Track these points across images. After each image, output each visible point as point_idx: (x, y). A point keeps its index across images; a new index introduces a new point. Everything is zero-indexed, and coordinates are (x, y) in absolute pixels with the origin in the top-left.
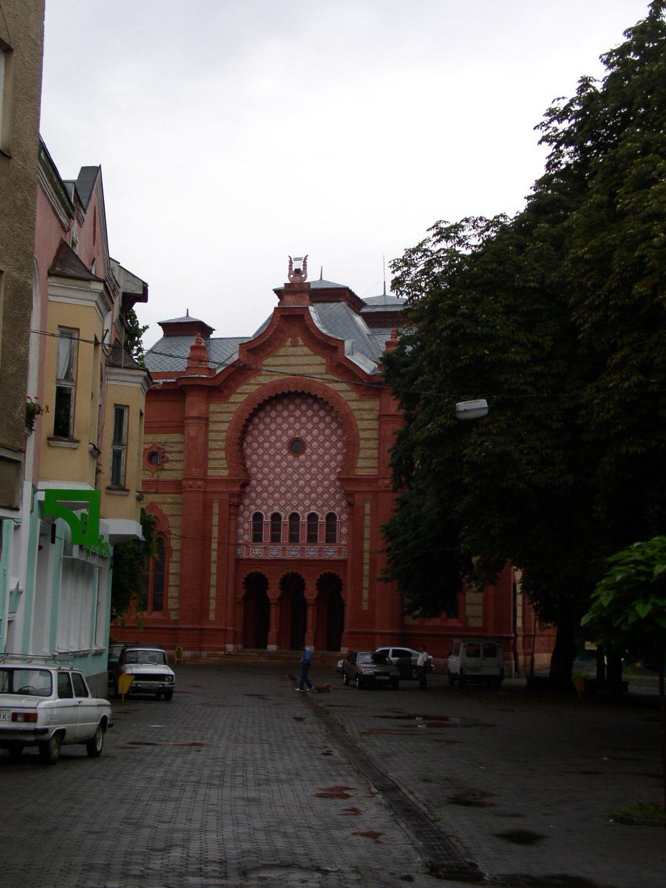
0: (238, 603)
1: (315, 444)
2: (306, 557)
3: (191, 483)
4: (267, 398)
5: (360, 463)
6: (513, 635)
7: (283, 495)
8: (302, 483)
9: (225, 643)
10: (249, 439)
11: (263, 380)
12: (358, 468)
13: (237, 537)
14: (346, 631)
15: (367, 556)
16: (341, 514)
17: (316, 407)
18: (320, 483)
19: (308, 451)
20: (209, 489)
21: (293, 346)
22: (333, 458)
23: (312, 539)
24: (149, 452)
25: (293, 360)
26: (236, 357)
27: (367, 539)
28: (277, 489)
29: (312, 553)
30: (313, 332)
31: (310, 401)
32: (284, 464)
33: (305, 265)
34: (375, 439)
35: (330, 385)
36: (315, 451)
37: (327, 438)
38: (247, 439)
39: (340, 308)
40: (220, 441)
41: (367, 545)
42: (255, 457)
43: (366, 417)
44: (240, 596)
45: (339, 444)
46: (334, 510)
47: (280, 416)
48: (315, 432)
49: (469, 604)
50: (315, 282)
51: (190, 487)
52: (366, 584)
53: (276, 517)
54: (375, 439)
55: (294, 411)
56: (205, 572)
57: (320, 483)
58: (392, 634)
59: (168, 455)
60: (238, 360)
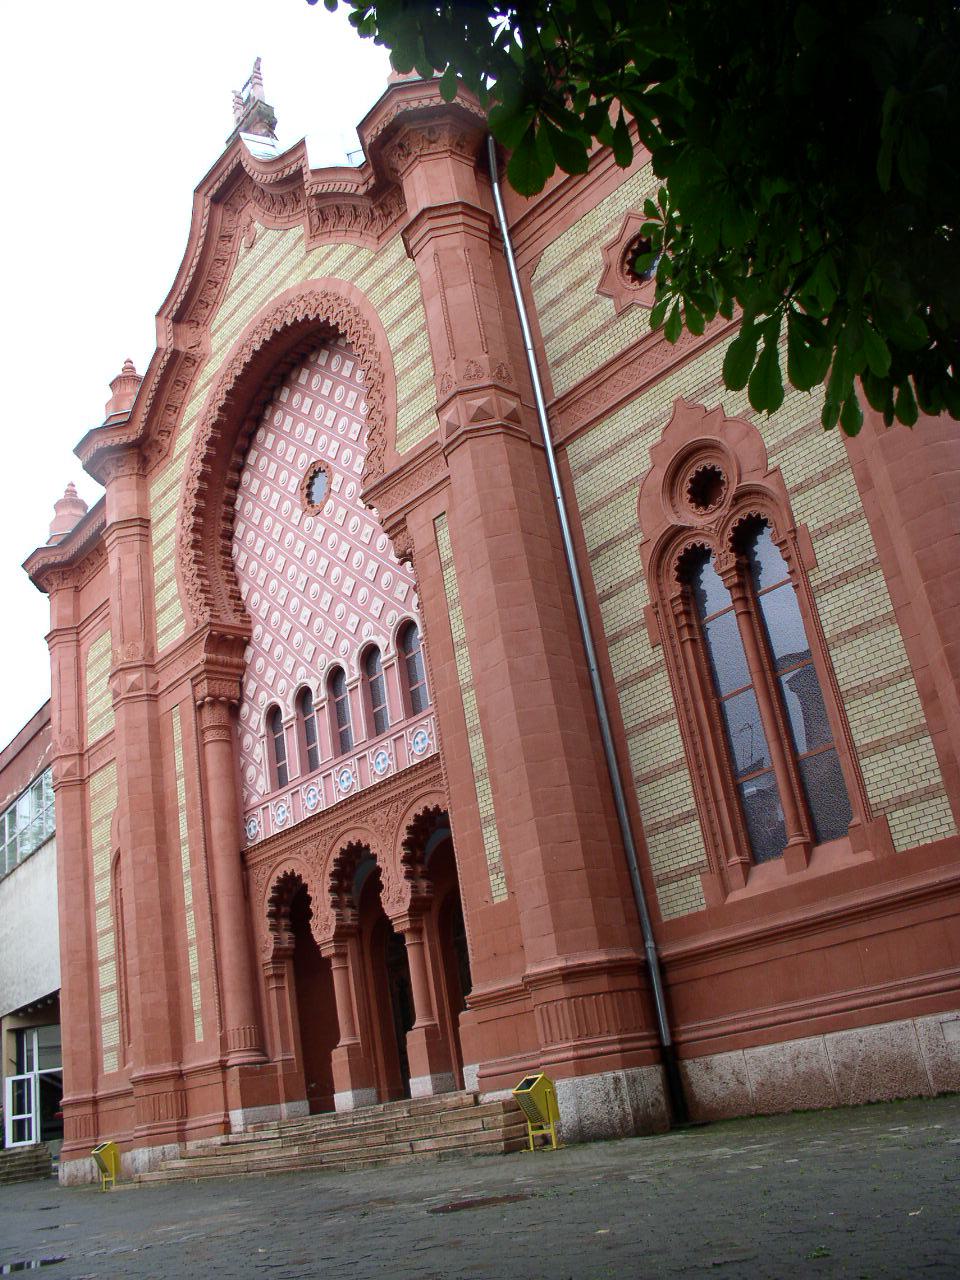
0: (268, 978)
10: (240, 529)
49: (877, 747)
56: (168, 912)
58: (568, 975)
60: (158, 350)
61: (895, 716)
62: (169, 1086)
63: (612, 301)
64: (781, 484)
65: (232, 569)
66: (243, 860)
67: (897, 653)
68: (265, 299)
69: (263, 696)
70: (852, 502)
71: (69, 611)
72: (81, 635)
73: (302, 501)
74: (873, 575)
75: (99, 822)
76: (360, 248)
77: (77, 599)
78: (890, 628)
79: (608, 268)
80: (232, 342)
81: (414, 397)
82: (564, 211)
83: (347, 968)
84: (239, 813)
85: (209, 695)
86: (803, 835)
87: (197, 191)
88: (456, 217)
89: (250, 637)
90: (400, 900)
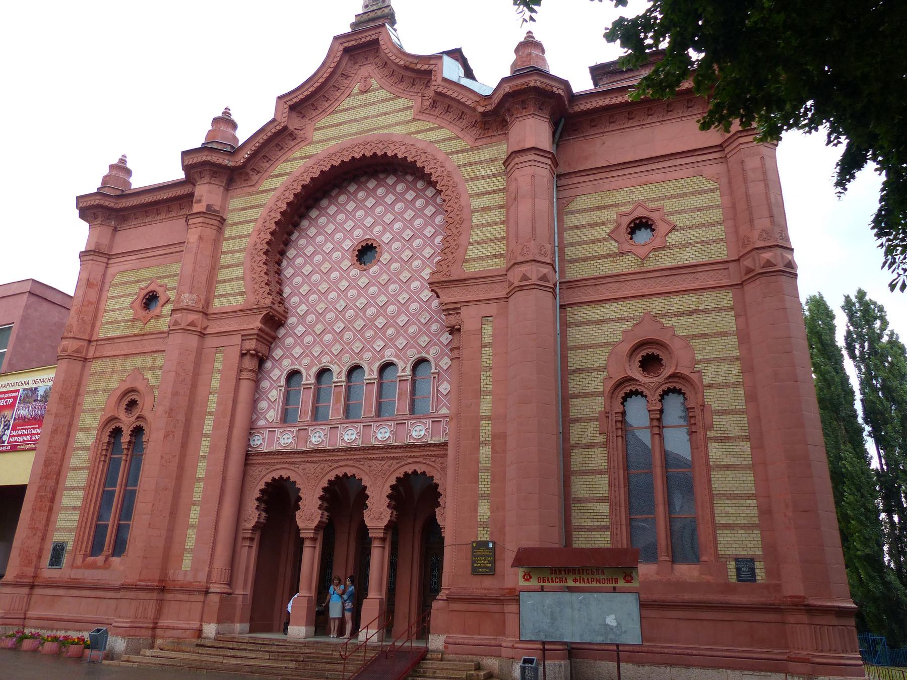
0: (244, 538)
1: (396, 245)
2: (374, 442)
5: (473, 252)
8: (371, 311)
10: (291, 253)
11: (310, 150)
12: (466, 261)
14: (442, 595)
15: (486, 428)
16: (439, 357)
17: (400, 187)
19: (385, 257)
20: (208, 331)
21: (363, 92)
24: (145, 292)
25: (361, 113)
27: (488, 393)
29: (383, 434)
30: (393, 58)
34: (501, 207)
35: (420, 136)
41: (486, 406)
42: (298, 279)
43: (483, 173)
45: (438, 239)
46: (428, 353)
49: (727, 527)
52: (484, 486)
54: (501, 207)
60: (273, 120)
61: (742, 515)
63: (617, 244)
64: (701, 379)
65: (279, 275)
66: (249, 457)
67: (749, 485)
68: (370, 130)
70: (740, 405)
71: (105, 241)
72: (111, 261)
73: (352, 257)
74: (744, 443)
75: (95, 392)
76: (458, 138)
77: (113, 235)
78: (748, 472)
79: (619, 226)
80: (334, 142)
81: (483, 243)
82: (598, 181)
83: (315, 547)
84: (251, 429)
85: (254, 350)
86: (668, 556)
87: (336, 38)
88: (547, 159)
89: (285, 322)
90: (380, 519)
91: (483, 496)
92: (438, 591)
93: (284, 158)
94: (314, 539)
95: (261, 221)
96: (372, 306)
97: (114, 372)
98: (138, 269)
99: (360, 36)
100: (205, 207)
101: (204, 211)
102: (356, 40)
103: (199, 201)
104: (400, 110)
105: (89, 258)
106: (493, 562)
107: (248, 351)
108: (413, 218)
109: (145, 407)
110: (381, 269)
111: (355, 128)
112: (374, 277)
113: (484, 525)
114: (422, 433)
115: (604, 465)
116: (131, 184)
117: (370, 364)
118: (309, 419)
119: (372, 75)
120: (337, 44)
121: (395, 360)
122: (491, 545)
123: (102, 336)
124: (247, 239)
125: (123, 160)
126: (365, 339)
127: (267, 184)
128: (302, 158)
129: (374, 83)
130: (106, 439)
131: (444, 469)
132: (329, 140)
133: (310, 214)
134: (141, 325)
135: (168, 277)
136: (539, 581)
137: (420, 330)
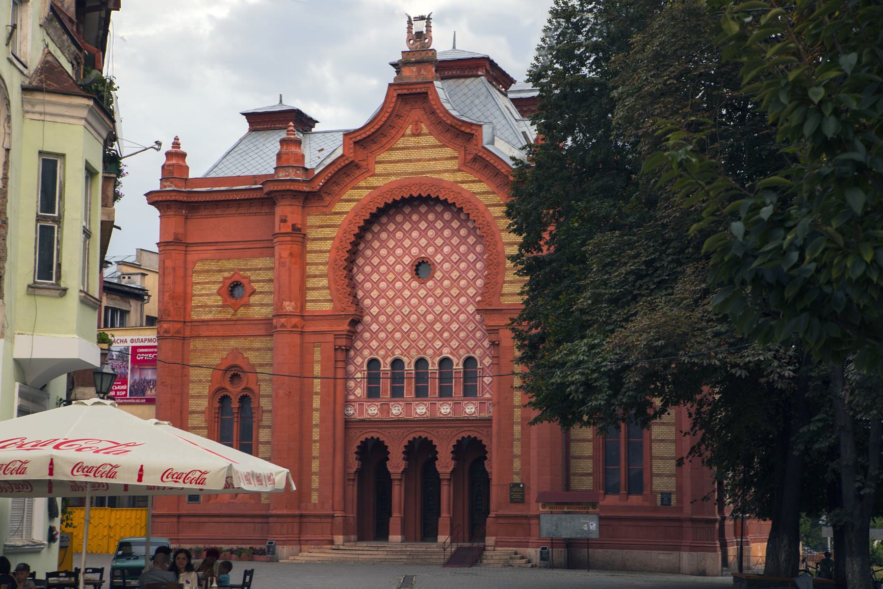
0: (348, 479)
1: (446, 266)
2: (438, 415)
3: (283, 320)
4: (382, 206)
6: (718, 517)
7: (406, 335)
8: (430, 317)
9: (332, 535)
10: (360, 261)
12: (503, 295)
13: (347, 391)
14: (492, 514)
16: (482, 357)
17: (447, 216)
18: (455, 317)
19: (438, 275)
20: (306, 329)
21: (414, 135)
22: (471, 283)
23: (445, 393)
24: (230, 281)
26: (339, 152)
28: (398, 328)
29: (445, 410)
30: (441, 115)
31: (439, 209)
32: (407, 293)
33: (428, 26)
36: (446, 276)
37: (463, 258)
38: (357, 262)
39: (479, 84)
40: (321, 264)
42: (368, 285)
44: (353, 469)
45: (479, 265)
46: (474, 353)
47: (400, 230)
48: (446, 249)
49: (658, 475)
50: (444, 53)
51: (283, 326)
52: (517, 450)
53: (397, 363)
55: (419, 222)
57: (455, 317)
59: (256, 286)
60: (343, 156)
62: (297, 520)
65: (351, 279)
68: (423, 173)
69: (366, 352)
72: (189, 249)
76: (493, 193)
80: (393, 178)
81: (513, 283)
84: (347, 403)
90: (446, 467)
91: (516, 456)
92: (488, 512)
93: (351, 185)
94: (400, 480)
95: (337, 241)
96: (430, 313)
97: (213, 350)
98: (219, 260)
99: (411, 87)
100: (291, 226)
101: (290, 230)
102: (408, 89)
103: (284, 221)
104: (447, 159)
105: (171, 248)
106: (523, 496)
107: (340, 347)
108: (459, 245)
109: (247, 381)
110: (436, 284)
111: (410, 168)
112: (430, 290)
113: (517, 474)
114: (473, 410)
115: (591, 436)
116: (187, 168)
117: (432, 358)
118: (389, 396)
119: (422, 120)
120: (392, 89)
121: (450, 356)
122: (521, 486)
123: (195, 317)
124: (328, 255)
125: (176, 144)
126: (427, 339)
127: (339, 207)
128: (367, 188)
129: (425, 130)
130: (218, 405)
131: (490, 436)
132: (389, 175)
133: (373, 228)
134: (231, 311)
135: (249, 270)
136: (550, 508)
137: (468, 335)
